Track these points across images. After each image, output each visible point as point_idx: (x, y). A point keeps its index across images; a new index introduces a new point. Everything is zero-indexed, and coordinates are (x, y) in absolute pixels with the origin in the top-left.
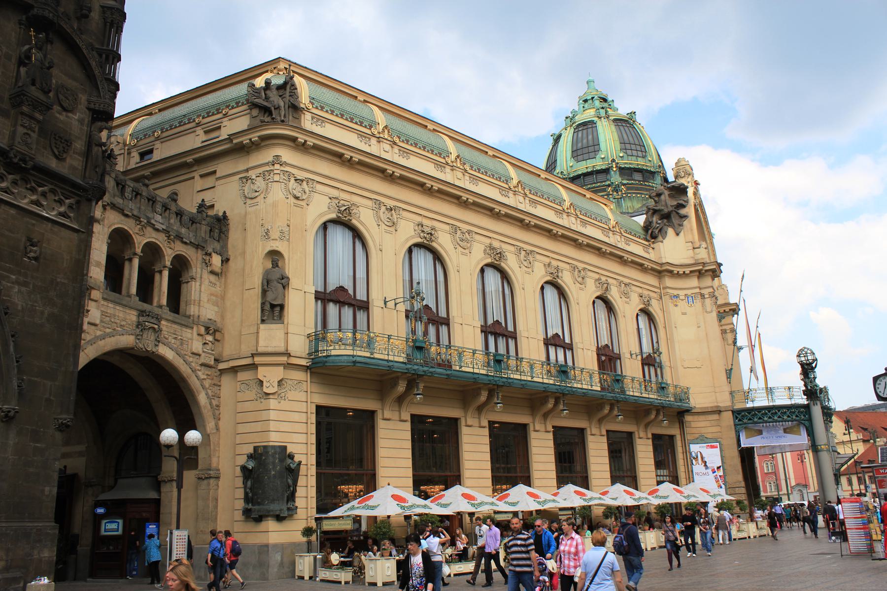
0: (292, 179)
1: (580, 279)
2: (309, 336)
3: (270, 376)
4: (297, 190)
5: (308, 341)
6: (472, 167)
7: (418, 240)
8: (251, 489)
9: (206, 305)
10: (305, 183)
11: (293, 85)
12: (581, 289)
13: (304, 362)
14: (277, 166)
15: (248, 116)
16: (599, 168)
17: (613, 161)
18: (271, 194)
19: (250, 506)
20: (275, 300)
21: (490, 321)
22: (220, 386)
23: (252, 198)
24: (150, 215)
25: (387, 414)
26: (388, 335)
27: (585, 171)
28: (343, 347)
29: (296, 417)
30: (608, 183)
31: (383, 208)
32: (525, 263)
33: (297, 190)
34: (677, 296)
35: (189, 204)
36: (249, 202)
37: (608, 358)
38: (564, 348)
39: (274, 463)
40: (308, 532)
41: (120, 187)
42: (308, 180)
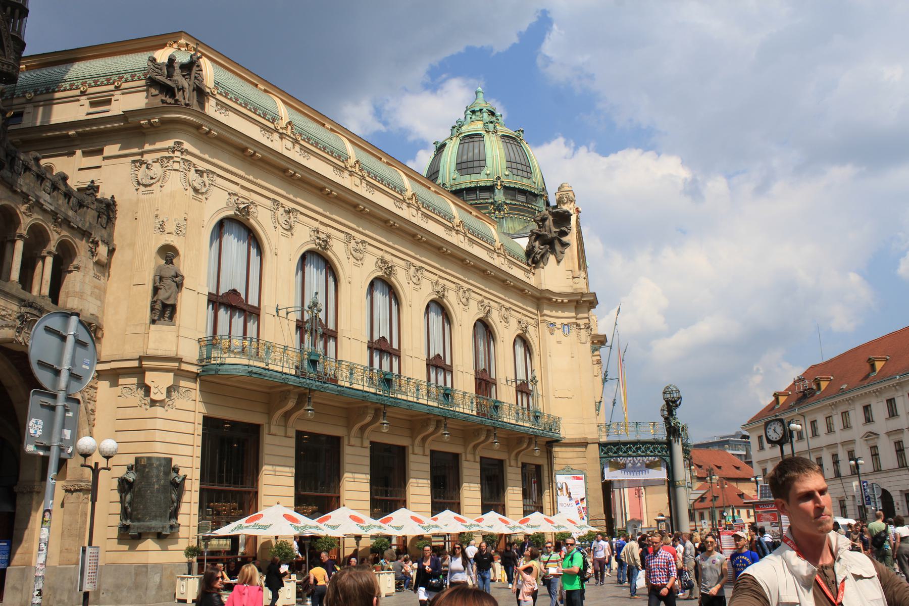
0: (193, 170)
1: (464, 300)
2: (199, 341)
3: (159, 382)
4: (197, 181)
5: (198, 346)
6: (369, 173)
7: (312, 246)
8: (130, 503)
9: (90, 299)
10: (205, 175)
11: (198, 66)
12: (465, 310)
13: (194, 369)
14: (178, 154)
15: (145, 94)
16: (483, 184)
17: (498, 178)
18: (169, 182)
19: (128, 522)
20: (168, 299)
21: (376, 338)
22: (96, 388)
23: (146, 186)
24: (38, 193)
25: (274, 429)
26: (278, 344)
27: (468, 186)
28: (232, 355)
29: (183, 427)
30: (490, 201)
31: (281, 210)
32: (414, 279)
33: (197, 181)
34: (553, 324)
35: (76, 181)
36: (142, 188)
37: (484, 382)
38: (444, 369)
39: (158, 476)
40: (191, 552)
41: (10, 158)
42: (209, 172)
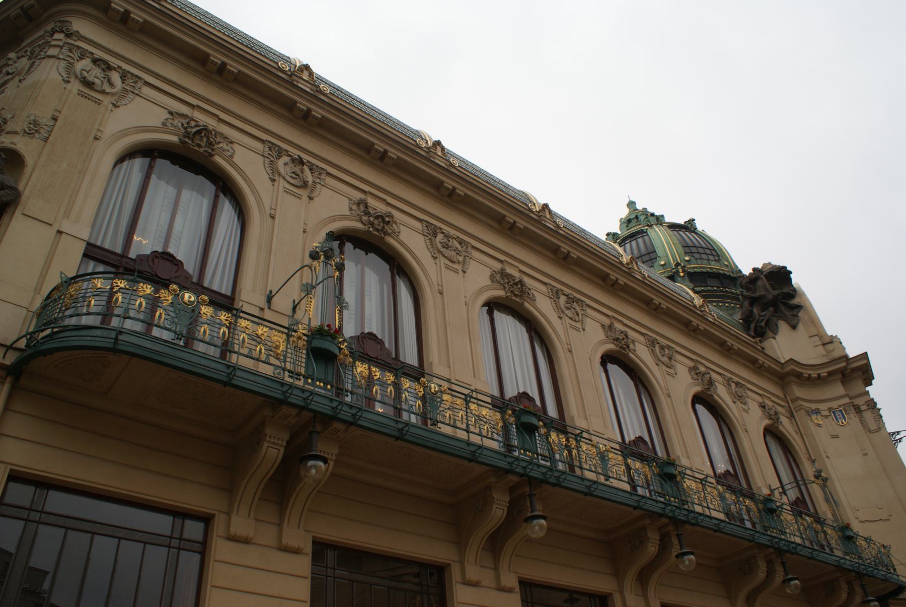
1: (665, 359)
4: (95, 74)
12: (669, 374)
17: (678, 264)
21: (510, 393)
25: (240, 524)
32: (567, 312)
